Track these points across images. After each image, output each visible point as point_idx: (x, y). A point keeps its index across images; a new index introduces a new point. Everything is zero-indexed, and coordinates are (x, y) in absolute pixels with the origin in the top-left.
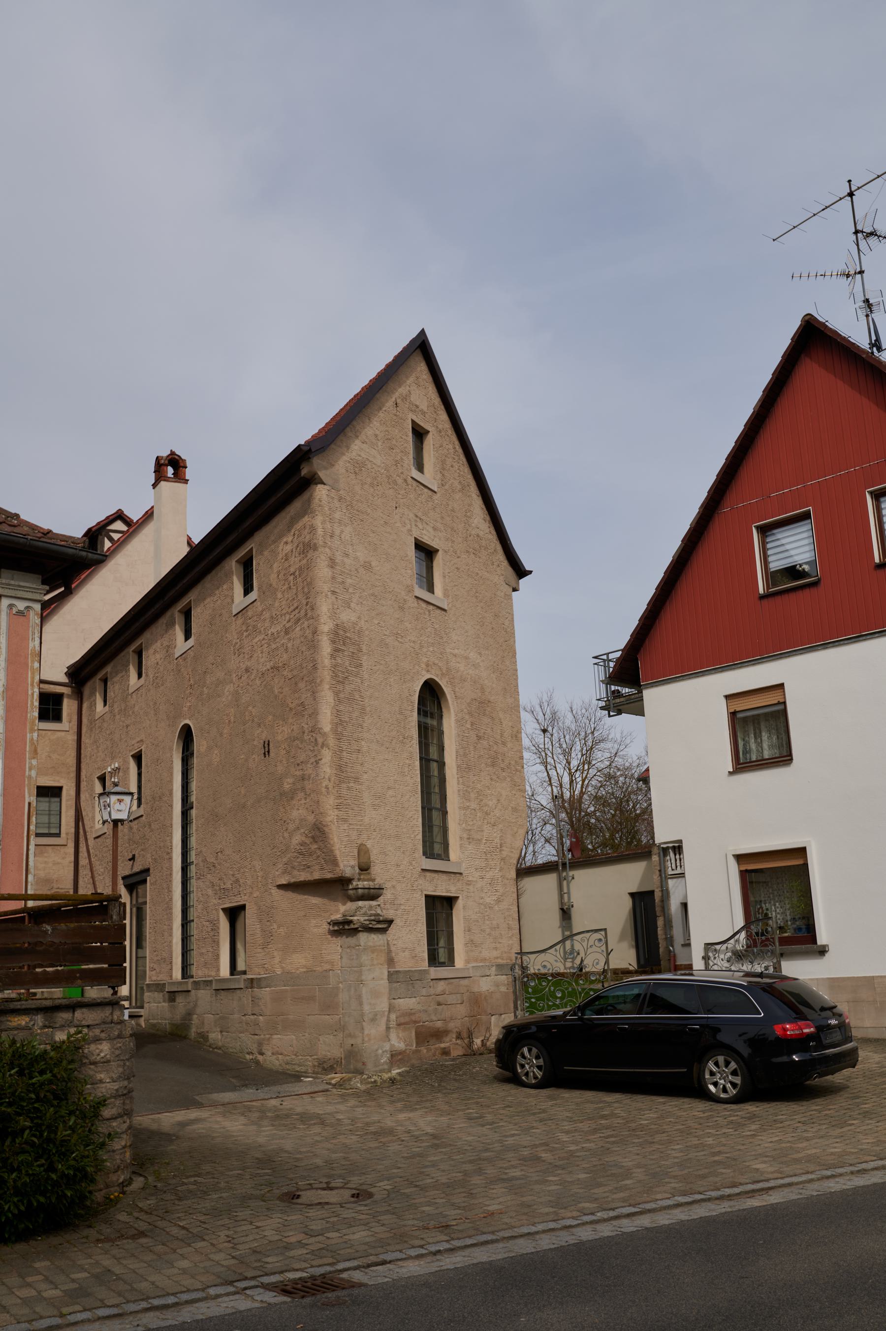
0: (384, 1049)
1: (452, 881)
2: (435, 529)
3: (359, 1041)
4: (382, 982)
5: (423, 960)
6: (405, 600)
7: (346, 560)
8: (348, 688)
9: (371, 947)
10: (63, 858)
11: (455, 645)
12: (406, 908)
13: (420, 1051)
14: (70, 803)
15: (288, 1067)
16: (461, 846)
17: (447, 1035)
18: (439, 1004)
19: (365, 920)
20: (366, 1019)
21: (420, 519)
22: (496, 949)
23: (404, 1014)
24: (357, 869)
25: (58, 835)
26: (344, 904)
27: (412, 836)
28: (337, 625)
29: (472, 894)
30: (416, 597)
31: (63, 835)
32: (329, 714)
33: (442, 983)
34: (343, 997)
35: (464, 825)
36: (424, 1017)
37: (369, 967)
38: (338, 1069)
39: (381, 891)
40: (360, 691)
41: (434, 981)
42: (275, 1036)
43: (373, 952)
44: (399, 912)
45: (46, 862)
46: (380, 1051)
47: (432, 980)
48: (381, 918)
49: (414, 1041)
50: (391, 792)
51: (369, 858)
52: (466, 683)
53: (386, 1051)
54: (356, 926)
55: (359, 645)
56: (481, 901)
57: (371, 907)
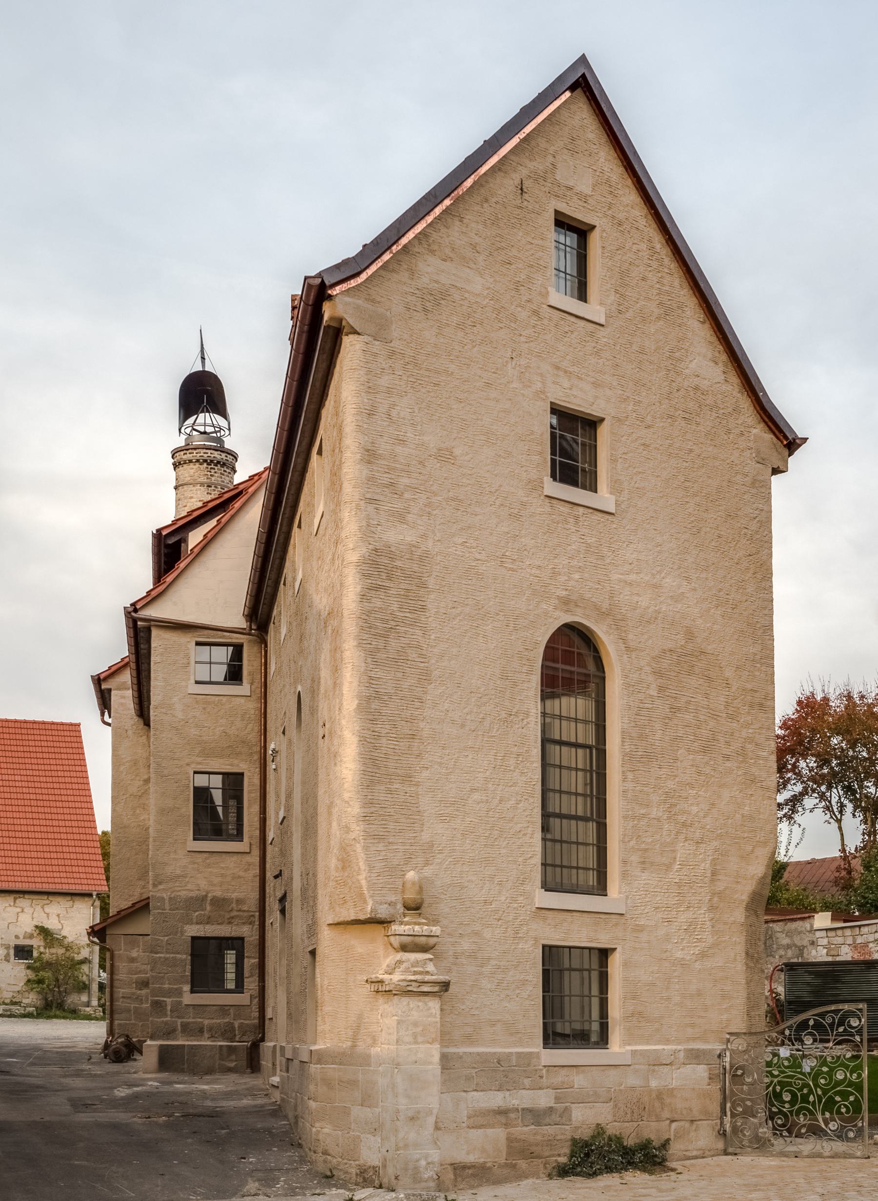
0: (430, 1160)
2: (596, 385)
6: (522, 504)
7: (399, 449)
8: (394, 644)
10: (246, 871)
12: (502, 963)
14: (253, 795)
21: (566, 372)
22: (693, 1025)
24: (400, 906)
27: (520, 859)
28: (376, 550)
30: (546, 496)
40: (419, 647)
44: (487, 970)
45: (222, 875)
46: (423, 1163)
50: (476, 796)
53: (432, 1163)
55: (420, 578)
56: (664, 956)
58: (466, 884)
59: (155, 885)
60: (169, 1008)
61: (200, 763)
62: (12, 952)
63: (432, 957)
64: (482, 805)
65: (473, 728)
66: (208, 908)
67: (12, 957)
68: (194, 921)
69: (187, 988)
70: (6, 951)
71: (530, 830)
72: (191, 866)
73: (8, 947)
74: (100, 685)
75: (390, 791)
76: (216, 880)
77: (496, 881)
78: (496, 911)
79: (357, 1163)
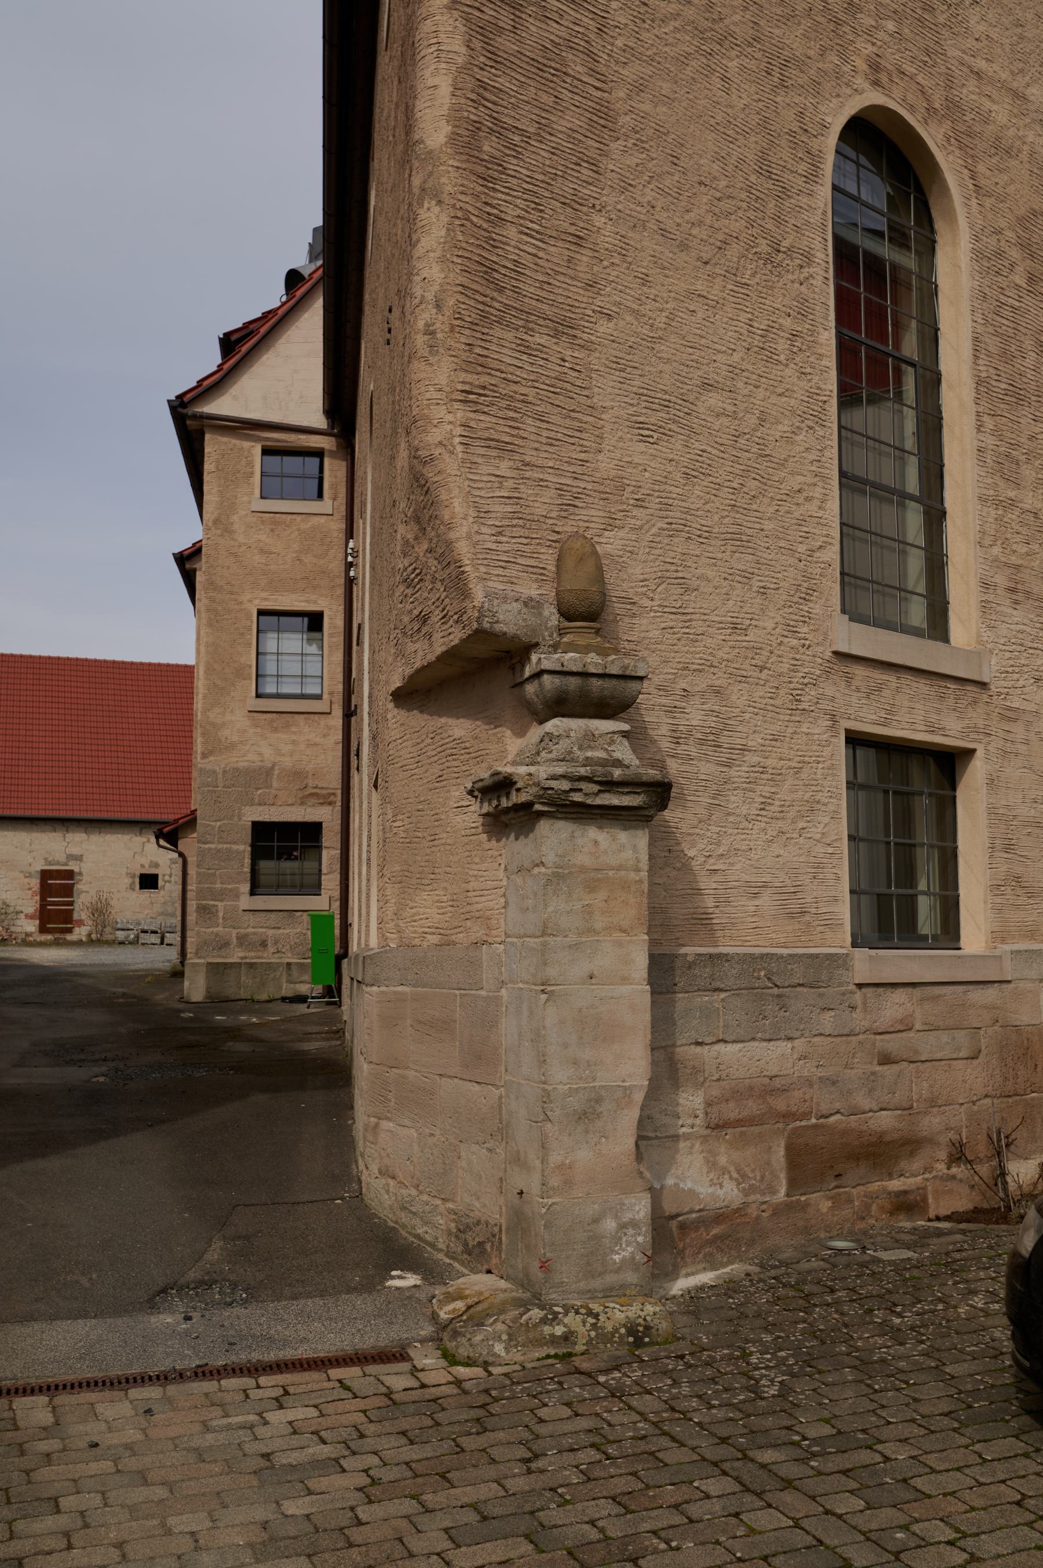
0: (627, 1216)
1: (951, 702)
3: (533, 1184)
4: (625, 989)
5: (833, 925)
9: (583, 869)
10: (325, 736)
11: (975, 43)
12: (769, 762)
13: (804, 1207)
14: (334, 640)
15: (404, 1218)
16: (985, 607)
17: (912, 1154)
18: (886, 1060)
19: (554, 777)
20: (556, 1114)
23: (737, 1094)
24: (551, 616)
25: (318, 697)
26: (521, 733)
27: (802, 548)
29: (1022, 749)
31: (325, 696)
32: (445, 88)
33: (899, 996)
34: (508, 1029)
35: (996, 550)
36: (825, 1100)
37: (572, 939)
38: (495, 1261)
39: (634, 685)
41: (869, 992)
42: (385, 1125)
43: (591, 887)
45: (294, 742)
46: (610, 1225)
47: (860, 986)
48: (617, 773)
49: (783, 1176)
50: (713, 400)
51: (599, 577)
52: (1013, 163)
53: (634, 1224)
54: (523, 798)
57: (590, 739)
58: (695, 583)
59: (204, 756)
60: (221, 914)
61: (265, 599)
62: (137, 880)
63: (626, 727)
64: (725, 421)
65: (705, 256)
66: (275, 784)
67: (138, 886)
68: (256, 801)
69: (246, 887)
70: (131, 880)
71: (818, 492)
72: (252, 731)
73: (133, 876)
74: (184, 565)
75: (525, 348)
76: (286, 748)
77: (756, 584)
78: (756, 650)
79: (451, 1205)
